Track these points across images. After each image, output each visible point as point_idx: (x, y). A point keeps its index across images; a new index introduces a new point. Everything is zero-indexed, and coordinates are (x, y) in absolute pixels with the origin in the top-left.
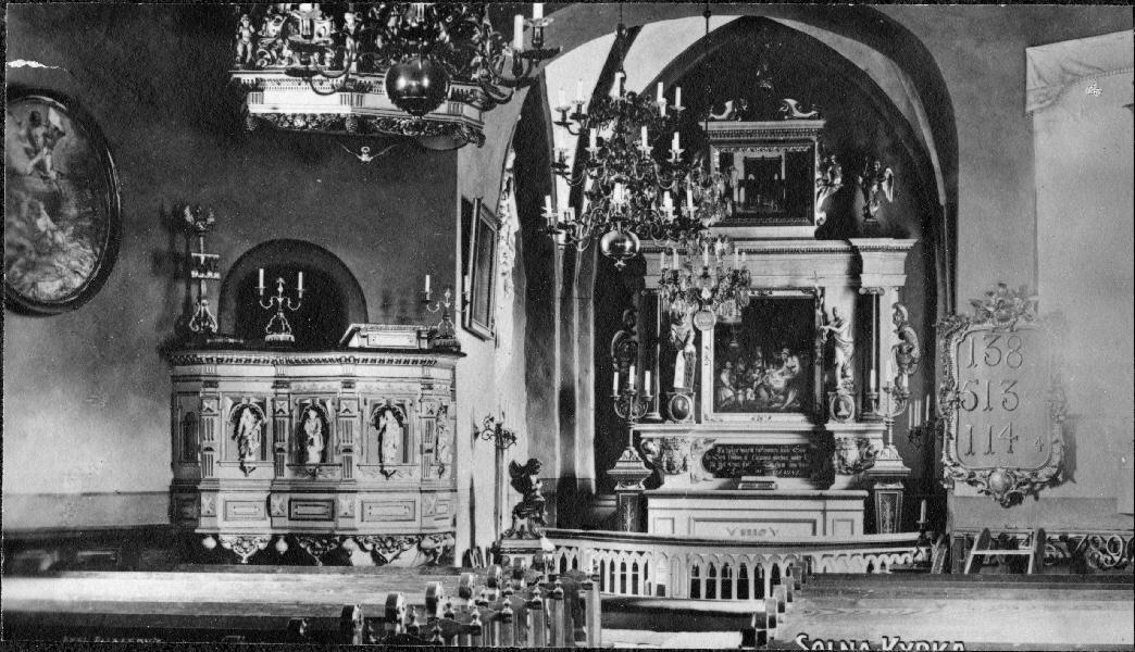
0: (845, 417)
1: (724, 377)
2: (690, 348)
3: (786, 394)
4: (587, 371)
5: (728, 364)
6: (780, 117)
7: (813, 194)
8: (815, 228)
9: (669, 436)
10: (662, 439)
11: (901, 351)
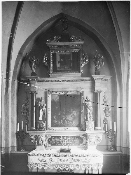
0: (91, 129)
1: (54, 117)
2: (44, 108)
4: (14, 116)
5: (56, 113)
6: (70, 41)
7: (80, 63)
8: (81, 74)
9: (37, 134)
10: (36, 135)
11: (106, 109)
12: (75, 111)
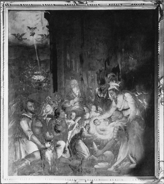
1: (25, 125)
3: (116, 151)
12: (128, 95)
